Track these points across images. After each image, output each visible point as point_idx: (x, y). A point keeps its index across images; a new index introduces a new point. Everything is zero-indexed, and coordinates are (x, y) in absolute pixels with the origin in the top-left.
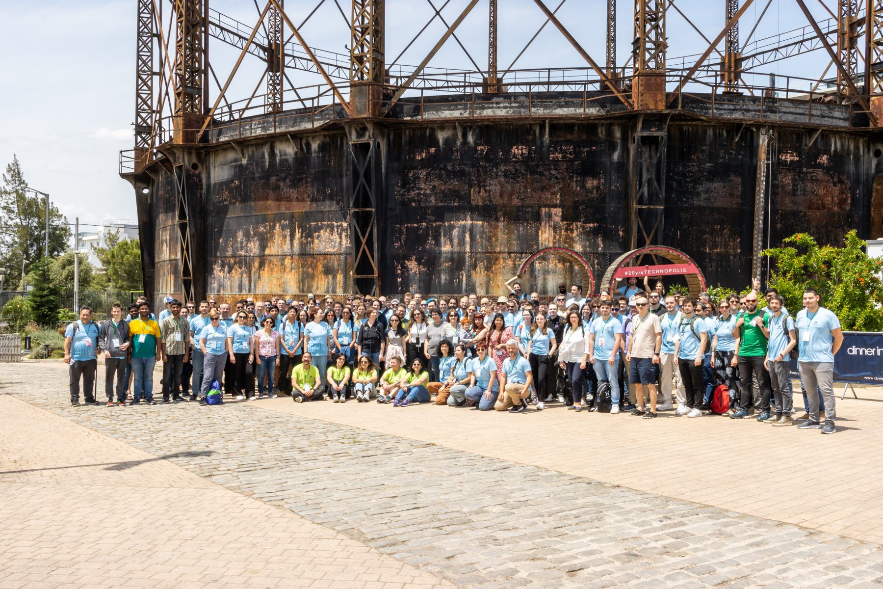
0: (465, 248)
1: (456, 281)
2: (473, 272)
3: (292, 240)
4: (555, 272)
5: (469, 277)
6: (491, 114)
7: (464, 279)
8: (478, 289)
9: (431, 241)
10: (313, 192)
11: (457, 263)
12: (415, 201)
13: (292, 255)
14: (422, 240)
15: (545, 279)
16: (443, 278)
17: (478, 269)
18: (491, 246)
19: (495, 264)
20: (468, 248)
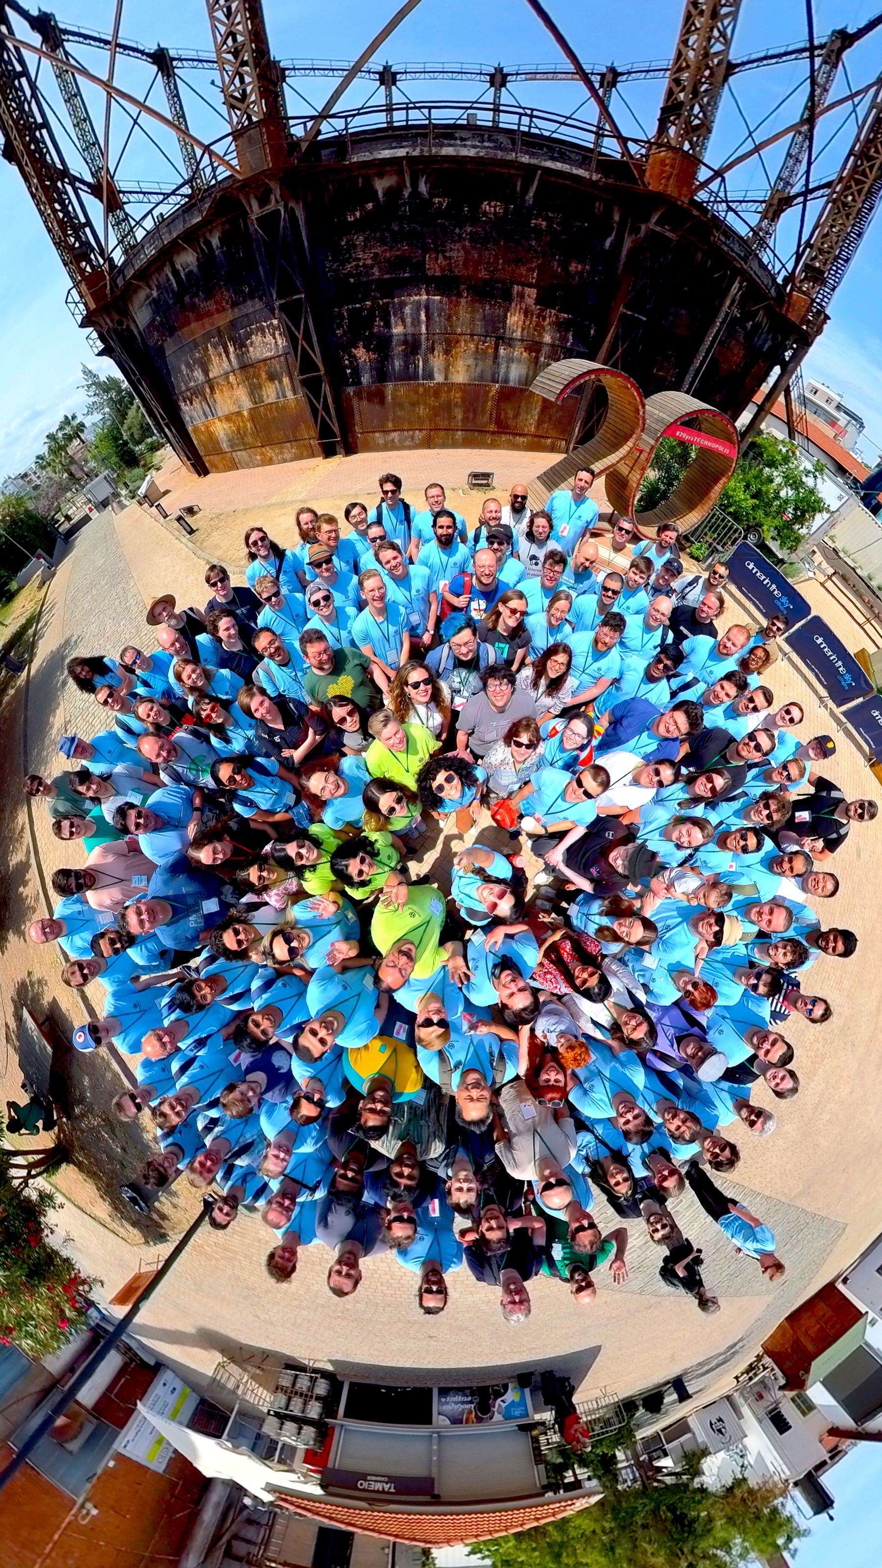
0: (420, 328)
1: (412, 367)
2: (430, 356)
3: (228, 356)
4: (519, 361)
5: (426, 362)
6: (454, 154)
7: (421, 364)
8: (436, 375)
9: (379, 322)
10: (231, 297)
11: (412, 346)
12: (353, 276)
13: (233, 371)
14: (369, 322)
15: (508, 367)
16: (398, 364)
17: (436, 353)
18: (451, 326)
19: (455, 347)
20: (423, 329)
